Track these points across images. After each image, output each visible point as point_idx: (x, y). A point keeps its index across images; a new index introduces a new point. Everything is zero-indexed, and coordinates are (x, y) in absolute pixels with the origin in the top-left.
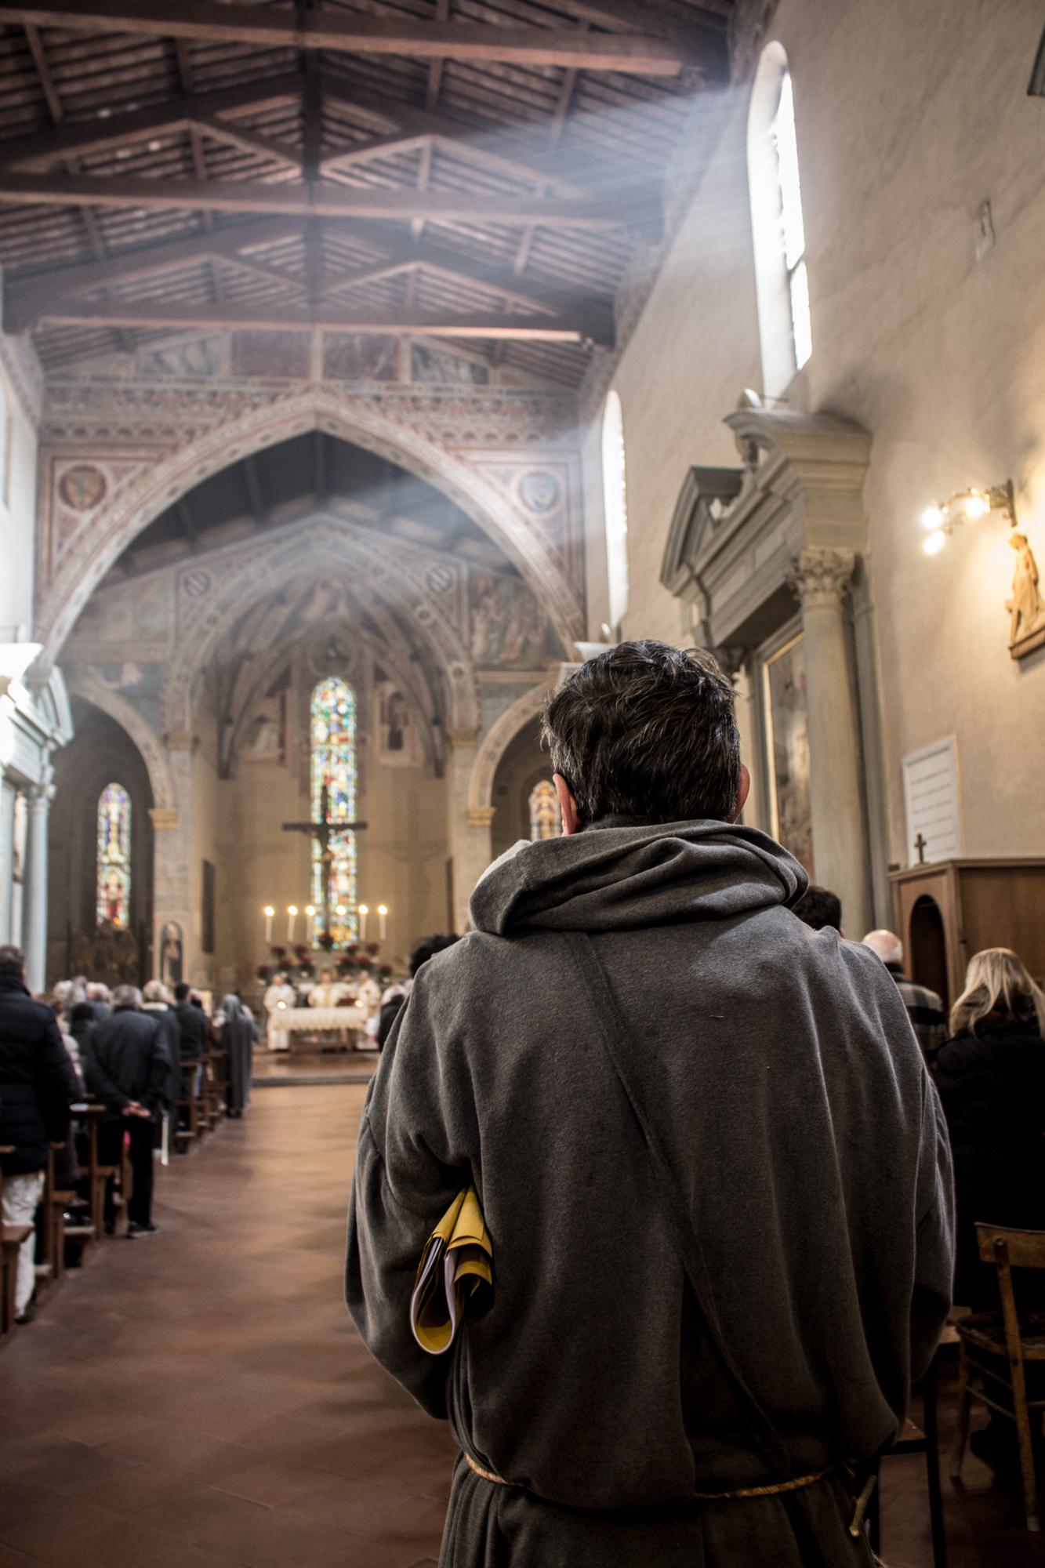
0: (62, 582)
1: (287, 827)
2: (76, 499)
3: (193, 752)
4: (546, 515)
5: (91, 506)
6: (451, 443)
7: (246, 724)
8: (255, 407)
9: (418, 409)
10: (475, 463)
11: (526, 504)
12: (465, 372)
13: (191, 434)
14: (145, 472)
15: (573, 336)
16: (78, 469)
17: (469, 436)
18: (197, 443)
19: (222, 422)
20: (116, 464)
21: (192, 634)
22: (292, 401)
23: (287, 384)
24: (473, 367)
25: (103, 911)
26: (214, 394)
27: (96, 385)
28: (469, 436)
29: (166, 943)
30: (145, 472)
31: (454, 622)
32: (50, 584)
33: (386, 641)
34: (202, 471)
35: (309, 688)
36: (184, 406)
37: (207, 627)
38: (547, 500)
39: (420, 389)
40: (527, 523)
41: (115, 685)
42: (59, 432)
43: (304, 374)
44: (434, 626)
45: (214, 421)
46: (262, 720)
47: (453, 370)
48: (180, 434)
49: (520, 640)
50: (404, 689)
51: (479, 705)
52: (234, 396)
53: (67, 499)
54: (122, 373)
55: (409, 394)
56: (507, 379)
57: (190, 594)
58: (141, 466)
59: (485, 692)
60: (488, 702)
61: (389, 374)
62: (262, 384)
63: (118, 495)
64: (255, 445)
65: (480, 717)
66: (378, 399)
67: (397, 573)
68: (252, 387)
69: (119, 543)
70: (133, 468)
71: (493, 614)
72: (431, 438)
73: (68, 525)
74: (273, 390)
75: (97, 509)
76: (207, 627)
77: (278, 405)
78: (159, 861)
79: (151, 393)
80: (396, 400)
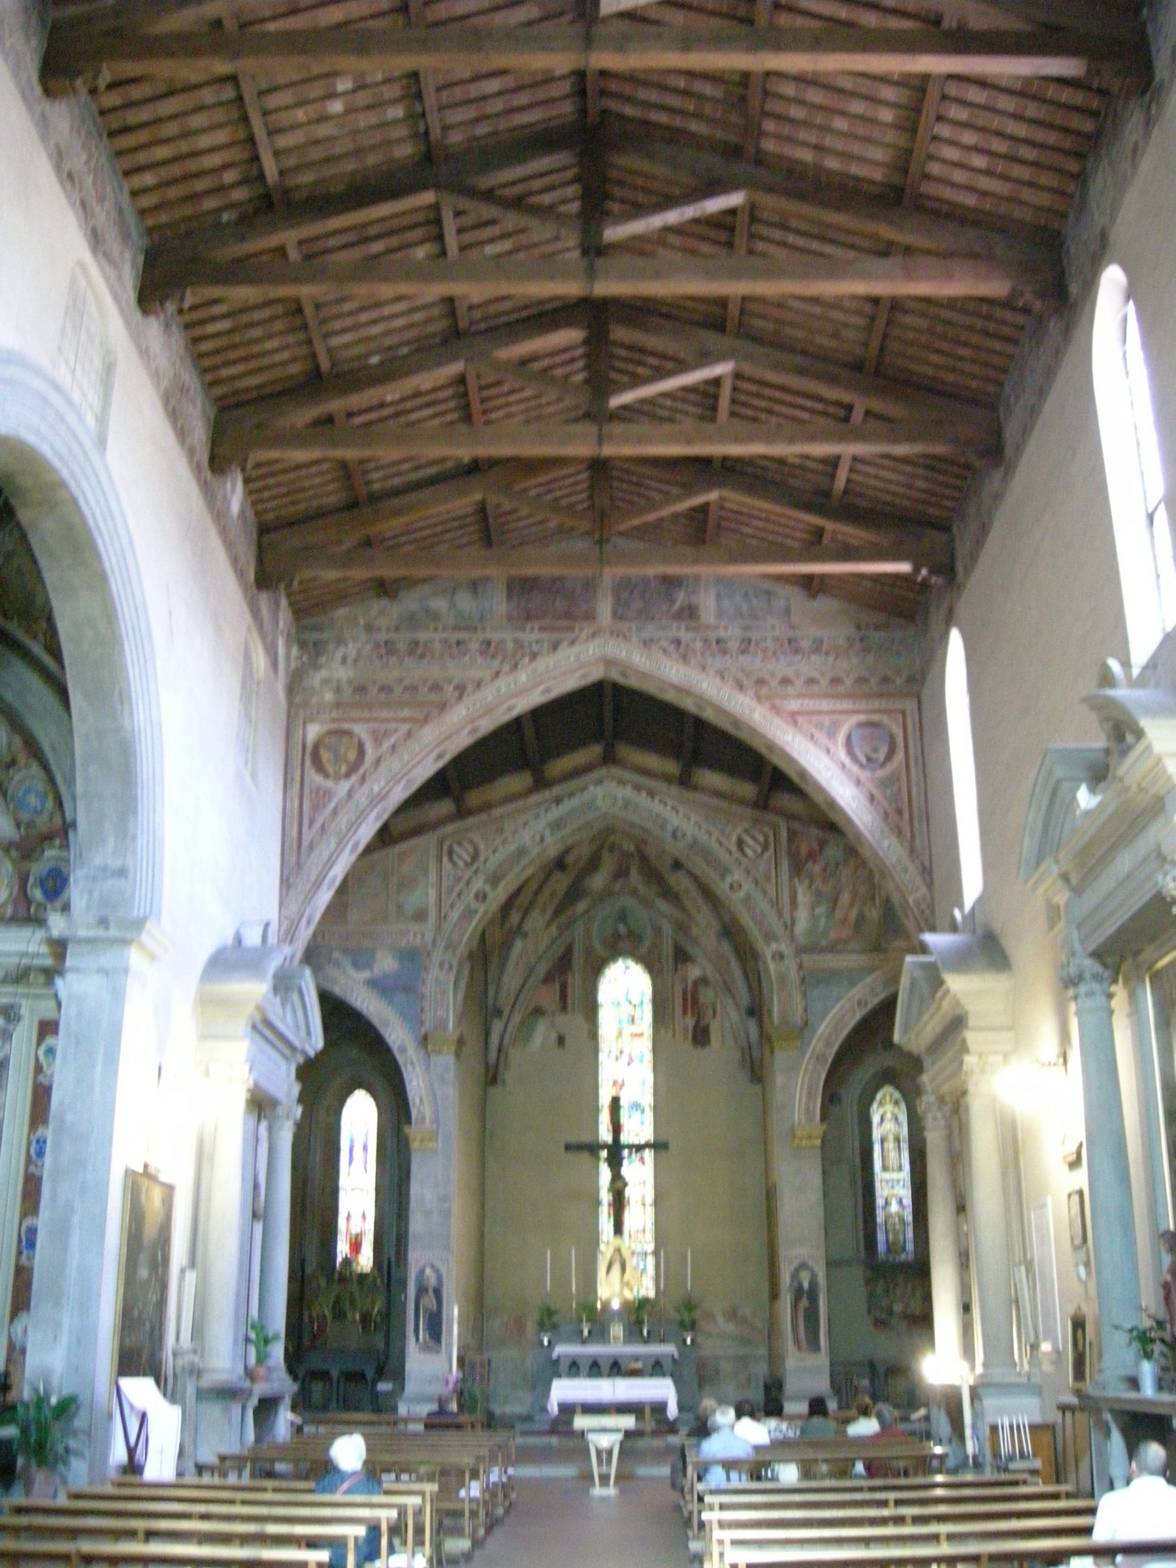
0: (313, 866)
1: (568, 1147)
2: (331, 770)
3: (458, 1055)
4: (881, 773)
5: (348, 775)
6: (764, 691)
7: (516, 1019)
8: (534, 656)
9: (724, 652)
13: (461, 690)
14: (409, 734)
15: (904, 567)
17: (786, 681)
18: (468, 700)
19: (497, 675)
20: (376, 725)
21: (455, 915)
22: (577, 648)
23: (572, 629)
25: (343, 1248)
26: (489, 643)
28: (786, 681)
29: (421, 1291)
30: (409, 734)
31: (772, 892)
32: (299, 865)
33: (689, 915)
34: (474, 731)
35: (596, 969)
36: (452, 657)
37: (474, 904)
40: (858, 782)
41: (366, 974)
43: (590, 616)
44: (747, 900)
45: (488, 675)
46: (538, 1012)
48: (449, 689)
49: (854, 914)
50: (709, 972)
51: (804, 994)
52: (510, 645)
53: (319, 767)
55: (713, 636)
57: (455, 864)
58: (404, 728)
59: (811, 980)
60: (816, 992)
61: (690, 613)
62: (541, 629)
63: (378, 762)
64: (536, 698)
65: (806, 1010)
67: (702, 837)
68: (530, 635)
69: (378, 818)
71: (818, 882)
72: (741, 687)
74: (555, 636)
75: (354, 778)
76: (474, 904)
78: (415, 1189)
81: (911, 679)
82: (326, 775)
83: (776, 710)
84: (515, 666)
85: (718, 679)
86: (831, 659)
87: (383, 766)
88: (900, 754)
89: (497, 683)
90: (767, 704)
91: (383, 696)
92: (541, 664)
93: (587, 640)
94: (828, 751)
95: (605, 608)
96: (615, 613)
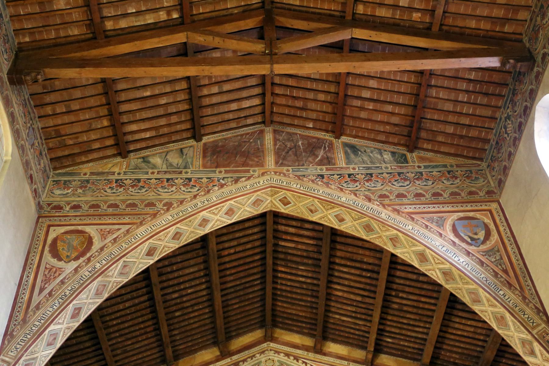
0: (35, 321)
4: (483, 247)
5: (77, 258)
6: (387, 201)
8: (222, 186)
9: (356, 181)
10: (409, 214)
11: (463, 240)
12: (387, 156)
13: (169, 206)
16: (66, 233)
17: (400, 196)
18: (172, 211)
19: (195, 197)
22: (252, 181)
23: (248, 171)
24: (393, 153)
26: (190, 180)
27: (94, 177)
28: (400, 196)
32: (24, 321)
34: (177, 236)
38: (481, 235)
39: (354, 169)
40: (468, 253)
42: (59, 208)
43: (261, 164)
45: (188, 196)
47: (379, 157)
52: (205, 180)
53: (55, 254)
54: (117, 170)
56: (422, 159)
58: (125, 228)
61: (328, 161)
62: (226, 172)
66: (322, 176)
68: (218, 174)
70: (119, 229)
72: (370, 200)
73: (53, 272)
74: (237, 175)
75: (81, 260)
77: (240, 185)
79: (139, 180)
80: (336, 177)
81: (489, 193)
82: (60, 259)
83: (398, 212)
84: (209, 191)
85: (353, 196)
86: (430, 183)
87: (106, 251)
88: (495, 237)
89: (194, 201)
90: (390, 208)
91: (110, 210)
92: (225, 190)
93: (259, 177)
94: (441, 235)
95: (270, 161)
96: (277, 163)
